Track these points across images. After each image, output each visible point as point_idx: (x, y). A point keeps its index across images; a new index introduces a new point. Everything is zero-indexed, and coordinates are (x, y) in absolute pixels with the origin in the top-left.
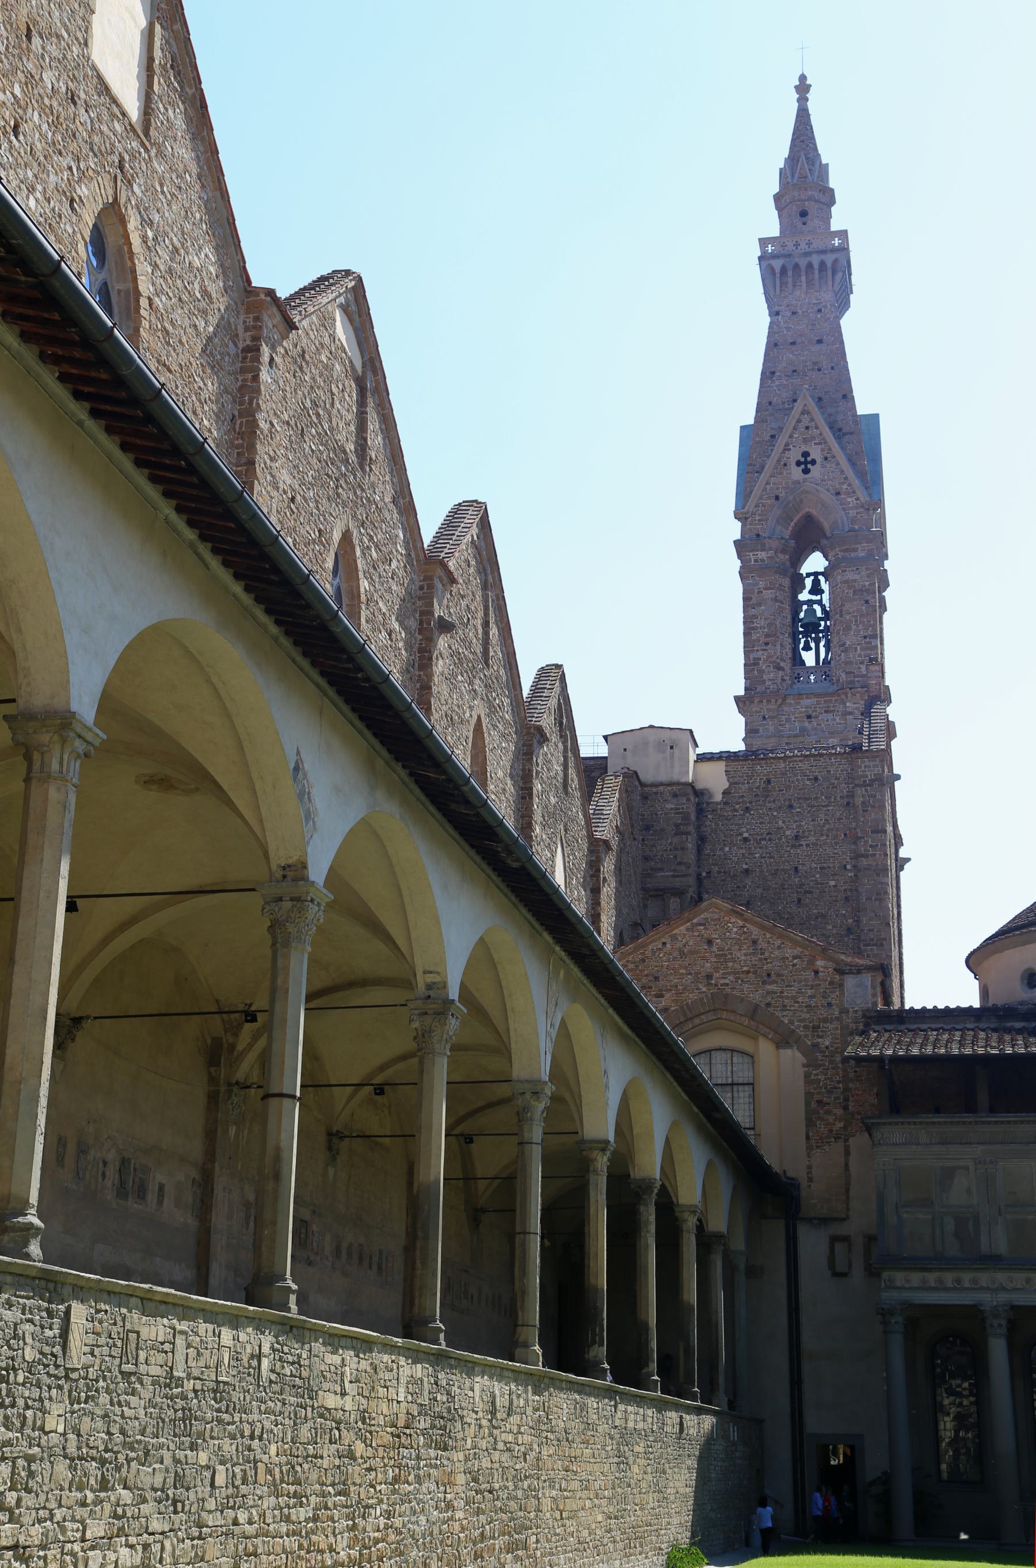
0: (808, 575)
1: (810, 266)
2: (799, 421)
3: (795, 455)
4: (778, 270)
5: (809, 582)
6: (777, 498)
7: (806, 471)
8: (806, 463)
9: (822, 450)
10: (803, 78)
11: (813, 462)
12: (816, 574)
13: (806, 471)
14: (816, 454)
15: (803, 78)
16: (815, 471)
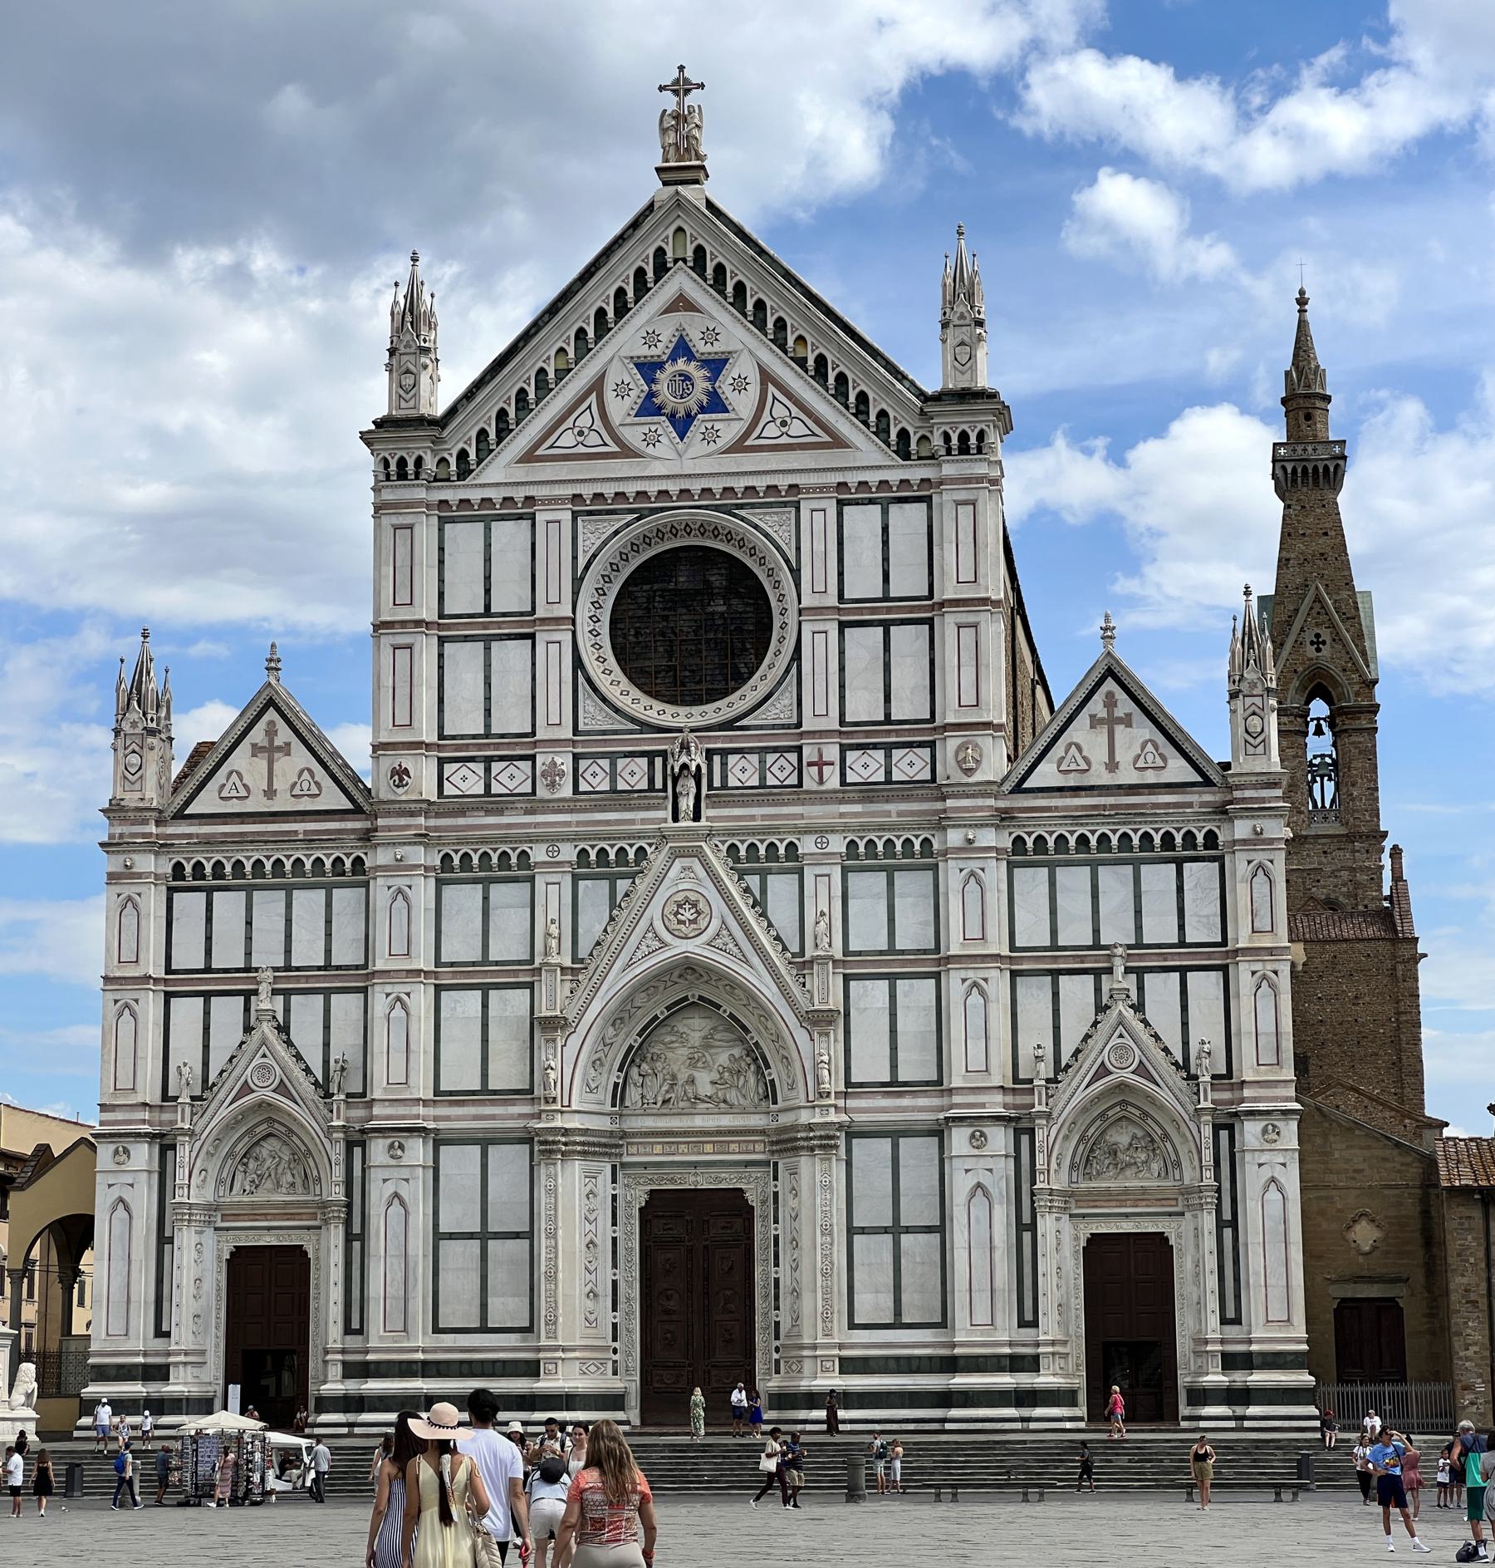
0: (1312, 720)
1: (1316, 468)
2: (1311, 608)
3: (1309, 636)
4: (1289, 471)
5: (1312, 727)
6: (1295, 671)
7: (1318, 650)
8: (1318, 643)
9: (1331, 633)
10: (1302, 292)
11: (1324, 643)
12: (1318, 719)
13: (1318, 650)
14: (1326, 635)
15: (1302, 292)
16: (1326, 651)
